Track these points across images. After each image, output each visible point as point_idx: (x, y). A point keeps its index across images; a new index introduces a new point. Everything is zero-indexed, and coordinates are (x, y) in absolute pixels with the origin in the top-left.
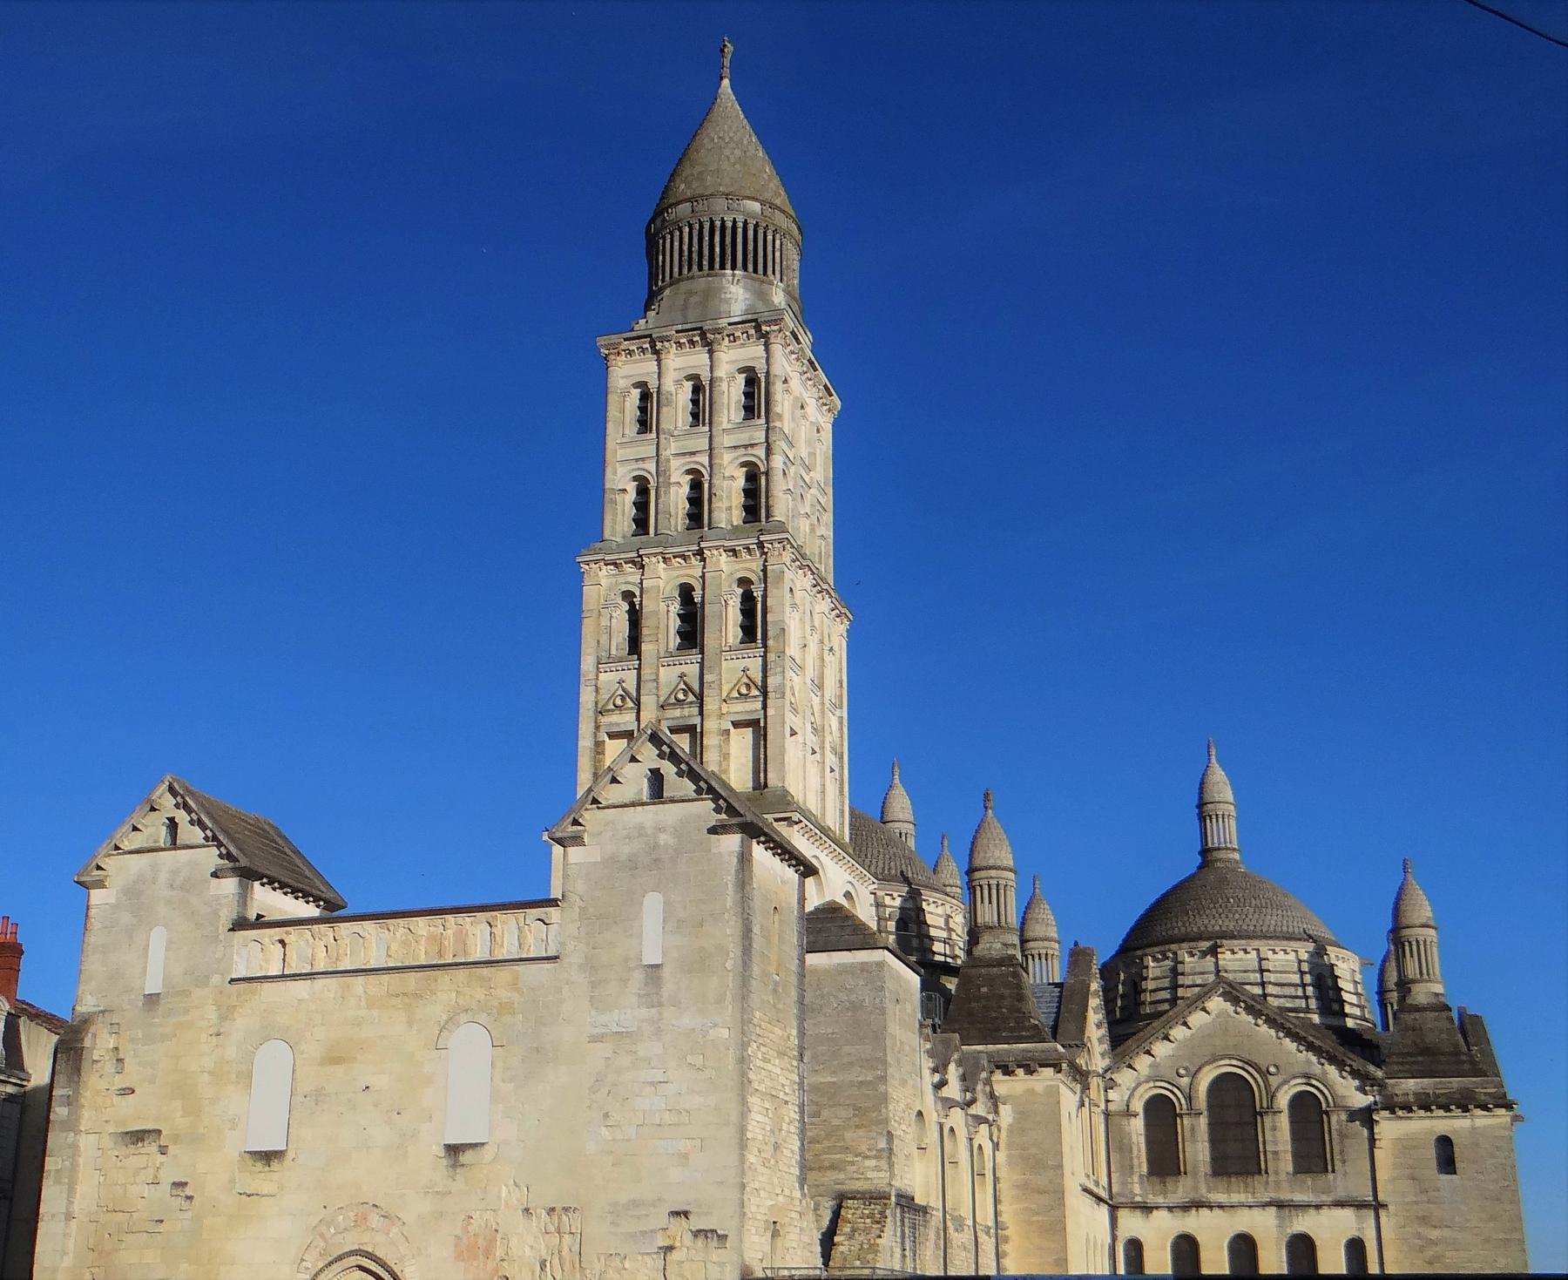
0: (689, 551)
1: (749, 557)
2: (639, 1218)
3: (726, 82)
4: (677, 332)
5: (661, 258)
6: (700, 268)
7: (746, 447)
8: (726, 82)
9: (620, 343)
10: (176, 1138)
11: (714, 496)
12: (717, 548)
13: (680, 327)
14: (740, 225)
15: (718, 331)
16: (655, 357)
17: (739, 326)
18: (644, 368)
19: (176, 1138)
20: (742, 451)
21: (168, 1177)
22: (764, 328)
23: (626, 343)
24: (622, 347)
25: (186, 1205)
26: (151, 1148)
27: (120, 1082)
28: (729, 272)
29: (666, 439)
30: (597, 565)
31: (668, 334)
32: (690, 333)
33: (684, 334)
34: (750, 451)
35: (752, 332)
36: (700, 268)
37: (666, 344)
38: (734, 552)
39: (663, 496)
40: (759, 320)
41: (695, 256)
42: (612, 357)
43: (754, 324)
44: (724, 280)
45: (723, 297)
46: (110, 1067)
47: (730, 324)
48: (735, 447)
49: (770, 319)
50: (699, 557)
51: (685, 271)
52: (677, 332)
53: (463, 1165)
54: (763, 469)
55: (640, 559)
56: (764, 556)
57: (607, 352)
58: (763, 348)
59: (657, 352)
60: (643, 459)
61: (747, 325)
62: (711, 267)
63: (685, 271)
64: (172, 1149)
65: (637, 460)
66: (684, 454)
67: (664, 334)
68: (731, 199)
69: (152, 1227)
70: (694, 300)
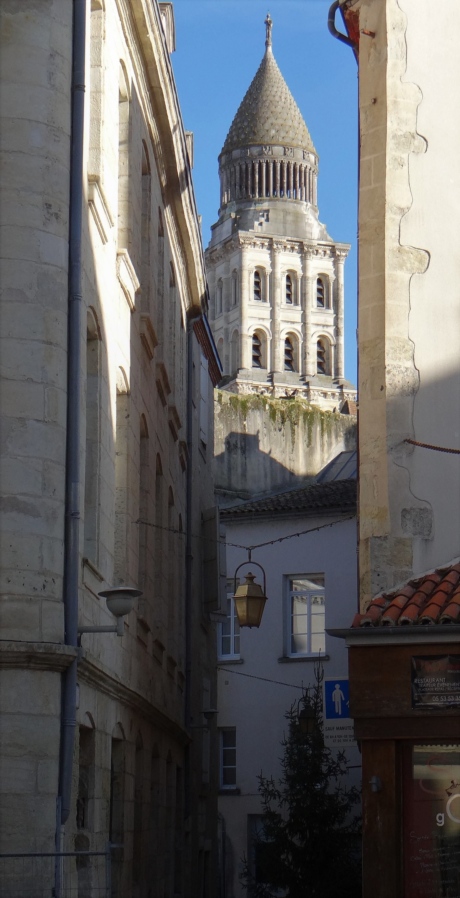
0: (301, 389)
1: (331, 399)
4: (287, 241)
5: (257, 177)
7: (324, 326)
9: (252, 238)
11: (308, 355)
12: (318, 391)
13: (290, 238)
14: (308, 170)
15: (311, 247)
16: (269, 252)
17: (323, 247)
20: (321, 328)
22: (338, 253)
23: (256, 239)
24: (253, 241)
28: (305, 203)
29: (279, 309)
30: (248, 386)
31: (283, 240)
32: (294, 243)
33: (290, 243)
34: (325, 329)
35: (328, 252)
37: (279, 246)
38: (325, 395)
39: (278, 347)
40: (336, 247)
42: (246, 246)
43: (331, 248)
44: (302, 207)
45: (306, 221)
47: (318, 244)
48: (318, 325)
49: (342, 248)
50: (304, 393)
52: (287, 241)
54: (332, 343)
55: (272, 388)
56: (341, 401)
57: (243, 241)
58: (332, 263)
59: (270, 247)
60: (263, 319)
61: (327, 247)
65: (260, 319)
66: (288, 322)
67: (280, 240)
68: (306, 152)
70: (290, 218)
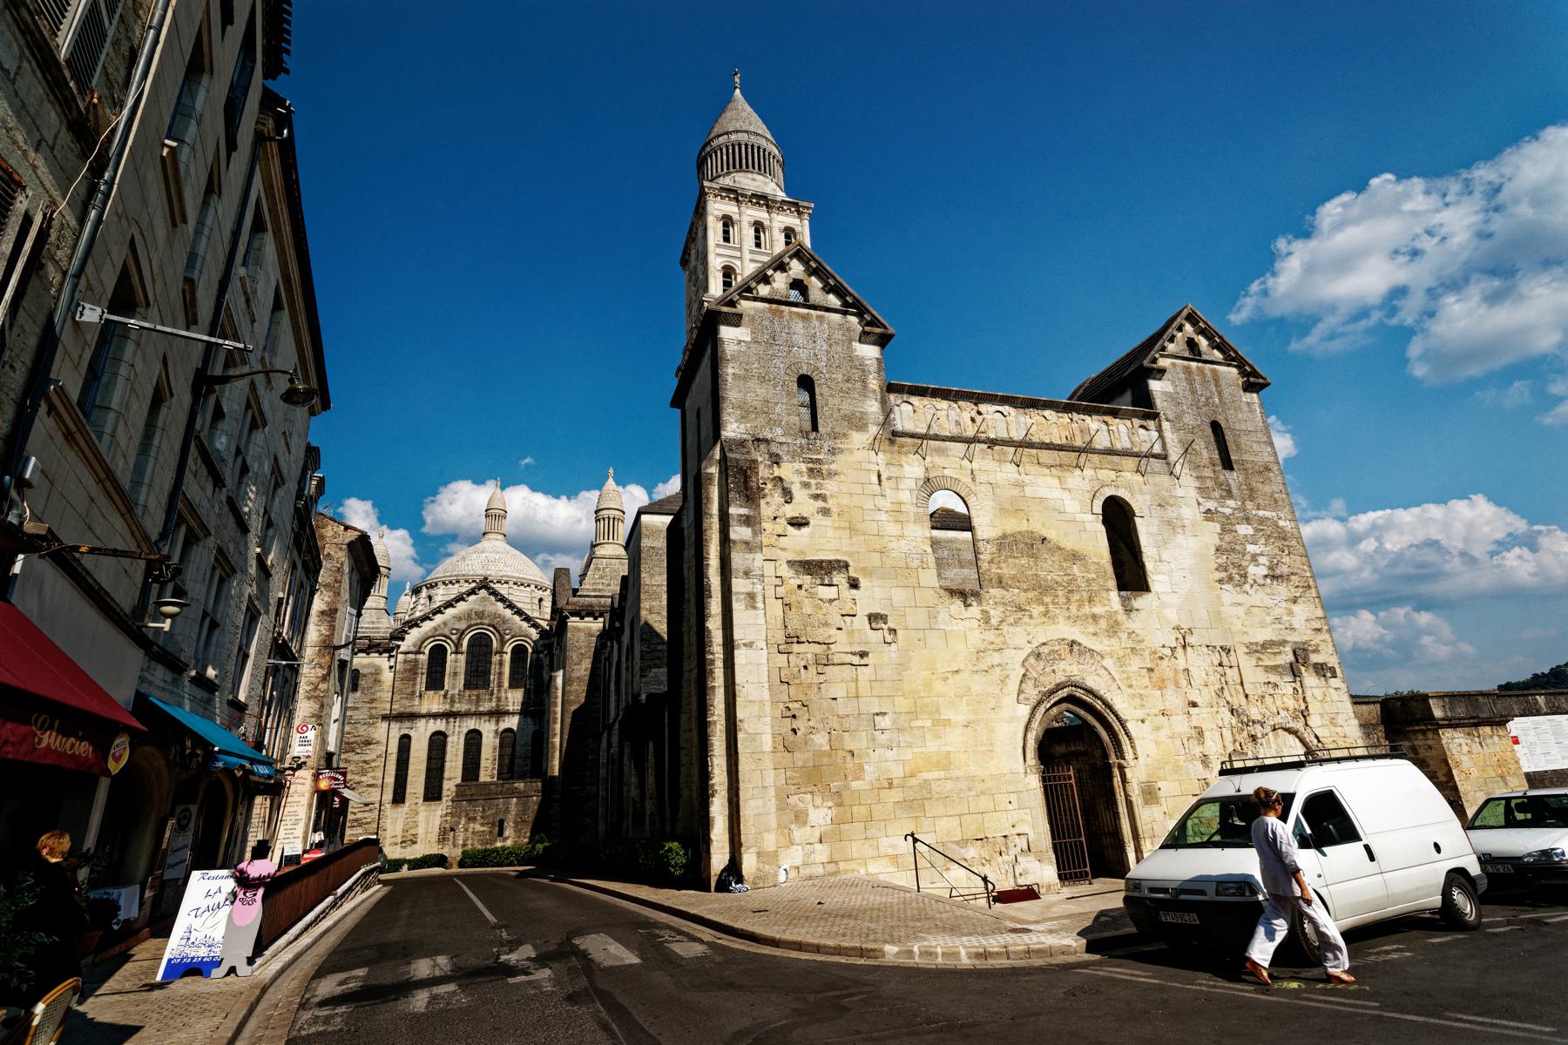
2: (1274, 653)
3: (738, 92)
6: (754, 168)
8: (738, 92)
10: (868, 572)
18: (730, 208)
19: (868, 572)
21: (863, 611)
25: (889, 638)
26: (839, 578)
27: (790, 511)
36: (754, 168)
41: (750, 161)
46: (777, 498)
51: (744, 167)
53: (1137, 610)
62: (759, 169)
63: (744, 167)
64: (863, 582)
69: (856, 660)
